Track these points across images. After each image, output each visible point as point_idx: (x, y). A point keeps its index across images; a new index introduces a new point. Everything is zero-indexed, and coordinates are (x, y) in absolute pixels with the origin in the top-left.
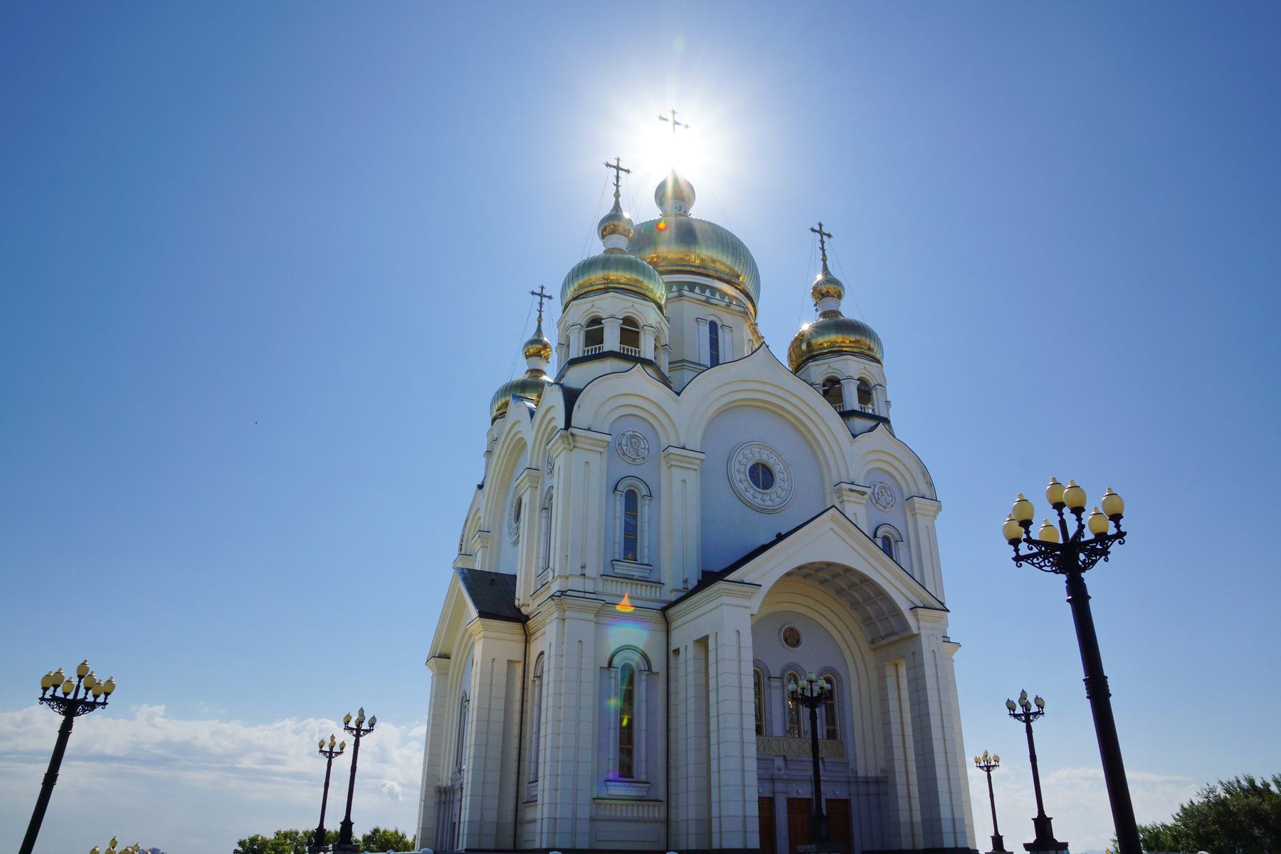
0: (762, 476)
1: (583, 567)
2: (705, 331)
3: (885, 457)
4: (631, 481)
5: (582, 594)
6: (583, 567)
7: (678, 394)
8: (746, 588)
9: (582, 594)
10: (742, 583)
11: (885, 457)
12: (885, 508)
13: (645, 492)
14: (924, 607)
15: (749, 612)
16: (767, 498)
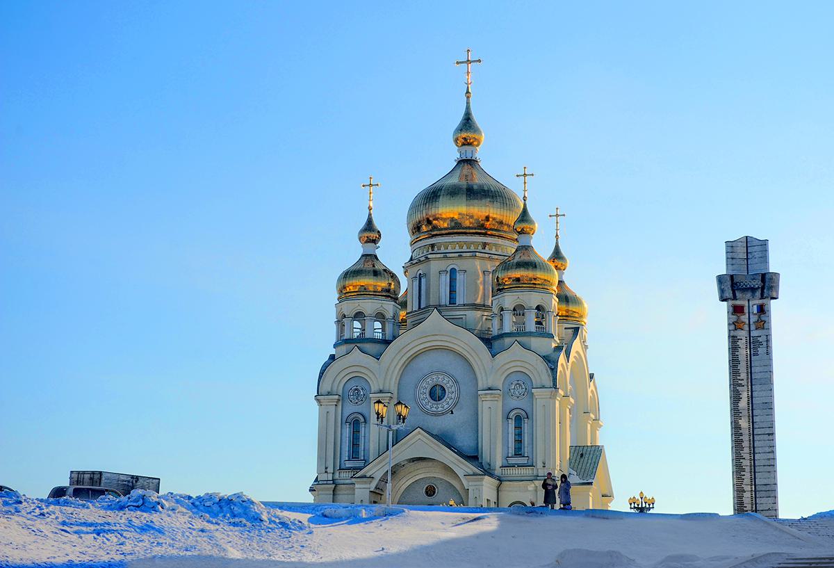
0: (437, 394)
1: (326, 468)
2: (445, 279)
3: (519, 363)
4: (355, 415)
5: (325, 482)
6: (326, 468)
7: (378, 359)
8: (365, 479)
9: (325, 482)
10: (365, 477)
11: (519, 363)
12: (518, 397)
13: (362, 420)
14: (475, 474)
15: (368, 490)
16: (440, 406)
